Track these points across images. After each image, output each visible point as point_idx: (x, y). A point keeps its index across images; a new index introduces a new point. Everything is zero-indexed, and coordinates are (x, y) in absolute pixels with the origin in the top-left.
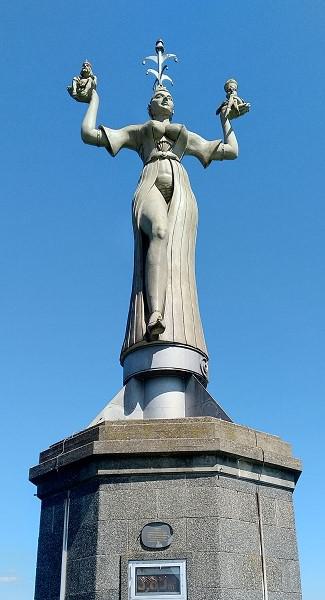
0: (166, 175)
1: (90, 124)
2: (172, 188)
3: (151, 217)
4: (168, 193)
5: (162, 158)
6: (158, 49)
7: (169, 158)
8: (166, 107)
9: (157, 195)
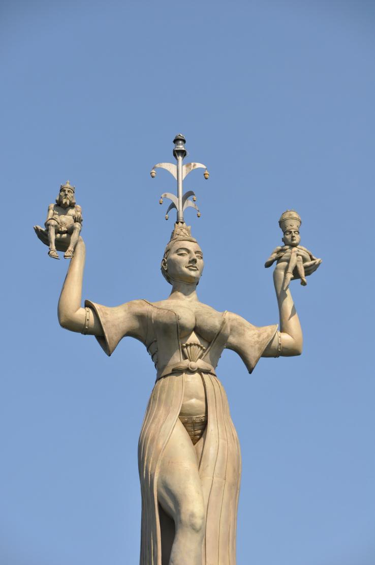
0: (193, 401)
1: (74, 293)
2: (204, 424)
3: (175, 488)
5: (189, 371)
6: (176, 153)
7: (200, 371)
8: (193, 273)
9: (178, 435)
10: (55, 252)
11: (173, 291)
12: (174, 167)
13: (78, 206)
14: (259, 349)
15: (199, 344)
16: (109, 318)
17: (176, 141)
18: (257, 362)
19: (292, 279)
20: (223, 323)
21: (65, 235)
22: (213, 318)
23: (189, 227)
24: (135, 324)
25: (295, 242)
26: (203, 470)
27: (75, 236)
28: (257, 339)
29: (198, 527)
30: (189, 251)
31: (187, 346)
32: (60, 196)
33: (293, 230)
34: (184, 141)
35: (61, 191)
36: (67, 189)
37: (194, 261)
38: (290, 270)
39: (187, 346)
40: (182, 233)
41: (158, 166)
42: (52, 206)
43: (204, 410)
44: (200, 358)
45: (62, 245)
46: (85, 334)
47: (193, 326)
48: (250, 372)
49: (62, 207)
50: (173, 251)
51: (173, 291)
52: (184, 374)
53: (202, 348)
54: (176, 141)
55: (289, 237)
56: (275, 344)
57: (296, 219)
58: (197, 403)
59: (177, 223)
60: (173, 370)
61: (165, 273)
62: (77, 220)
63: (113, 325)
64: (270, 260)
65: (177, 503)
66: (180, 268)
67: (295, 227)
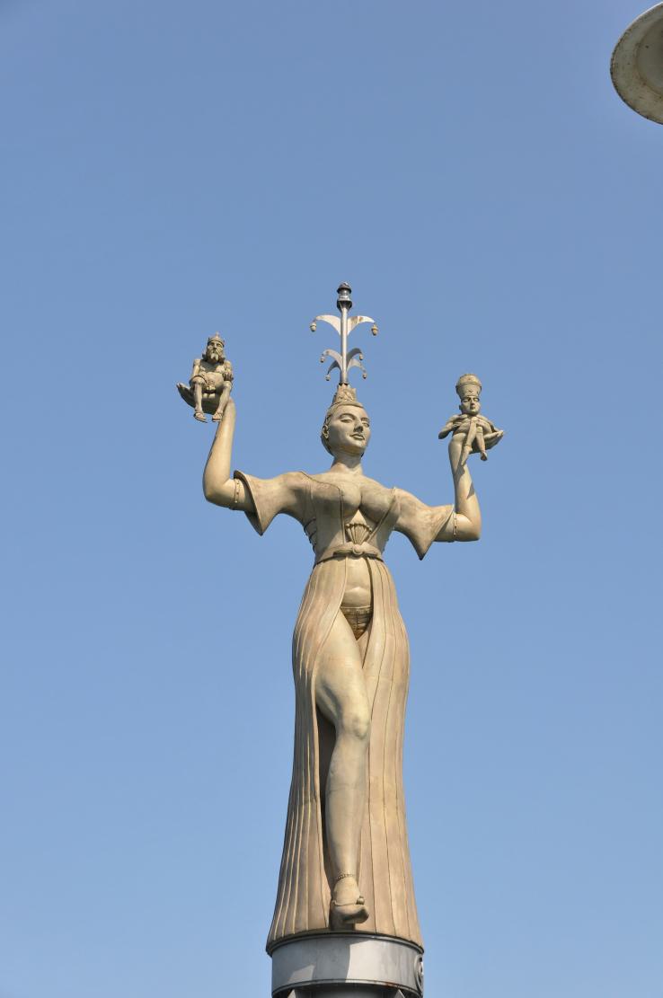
0: (357, 590)
1: (222, 462)
2: (369, 617)
3: (336, 688)
4: (361, 620)
5: (353, 555)
6: (341, 304)
7: (366, 556)
8: (358, 443)
9: (337, 629)
10: (201, 415)
11: (335, 463)
12: (338, 320)
13: (228, 362)
14: (432, 532)
15: (365, 524)
16: (263, 491)
17: (340, 290)
18: (429, 547)
19: (471, 453)
20: (394, 501)
21: (213, 395)
22: (381, 496)
23: (354, 390)
24: (292, 500)
25: (474, 410)
26: (367, 669)
27: (224, 397)
28: (429, 521)
29: (362, 734)
30: (354, 418)
31: (351, 526)
32: (208, 350)
33: (472, 397)
34: (350, 291)
35: (208, 344)
36: (216, 343)
37: (360, 429)
38: (469, 442)
39: (351, 526)
40: (346, 397)
41: (319, 318)
42: (198, 361)
43: (370, 601)
44: (366, 540)
45: (210, 407)
46: (234, 509)
47: (359, 504)
48: (421, 559)
49: (209, 362)
50: (335, 417)
51: (335, 463)
52: (347, 559)
53: (368, 529)
54: (340, 290)
55: (467, 404)
56: (450, 527)
57: (476, 384)
58: (361, 592)
59: (341, 384)
60: (335, 553)
61: (324, 440)
62: (226, 378)
63: (267, 500)
64: (445, 430)
65: (338, 706)
66: (343, 436)
67: (474, 393)
